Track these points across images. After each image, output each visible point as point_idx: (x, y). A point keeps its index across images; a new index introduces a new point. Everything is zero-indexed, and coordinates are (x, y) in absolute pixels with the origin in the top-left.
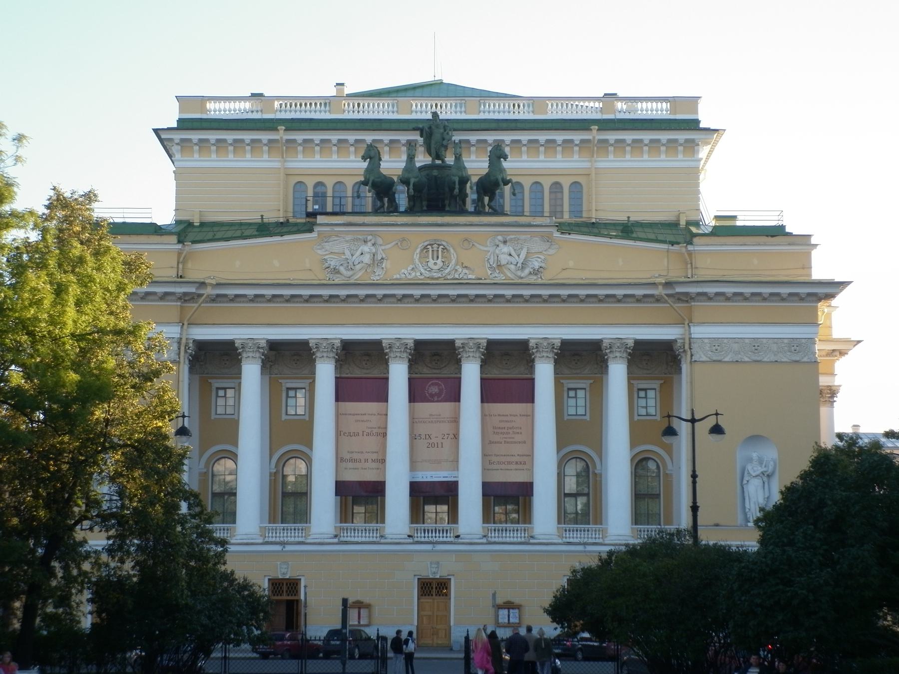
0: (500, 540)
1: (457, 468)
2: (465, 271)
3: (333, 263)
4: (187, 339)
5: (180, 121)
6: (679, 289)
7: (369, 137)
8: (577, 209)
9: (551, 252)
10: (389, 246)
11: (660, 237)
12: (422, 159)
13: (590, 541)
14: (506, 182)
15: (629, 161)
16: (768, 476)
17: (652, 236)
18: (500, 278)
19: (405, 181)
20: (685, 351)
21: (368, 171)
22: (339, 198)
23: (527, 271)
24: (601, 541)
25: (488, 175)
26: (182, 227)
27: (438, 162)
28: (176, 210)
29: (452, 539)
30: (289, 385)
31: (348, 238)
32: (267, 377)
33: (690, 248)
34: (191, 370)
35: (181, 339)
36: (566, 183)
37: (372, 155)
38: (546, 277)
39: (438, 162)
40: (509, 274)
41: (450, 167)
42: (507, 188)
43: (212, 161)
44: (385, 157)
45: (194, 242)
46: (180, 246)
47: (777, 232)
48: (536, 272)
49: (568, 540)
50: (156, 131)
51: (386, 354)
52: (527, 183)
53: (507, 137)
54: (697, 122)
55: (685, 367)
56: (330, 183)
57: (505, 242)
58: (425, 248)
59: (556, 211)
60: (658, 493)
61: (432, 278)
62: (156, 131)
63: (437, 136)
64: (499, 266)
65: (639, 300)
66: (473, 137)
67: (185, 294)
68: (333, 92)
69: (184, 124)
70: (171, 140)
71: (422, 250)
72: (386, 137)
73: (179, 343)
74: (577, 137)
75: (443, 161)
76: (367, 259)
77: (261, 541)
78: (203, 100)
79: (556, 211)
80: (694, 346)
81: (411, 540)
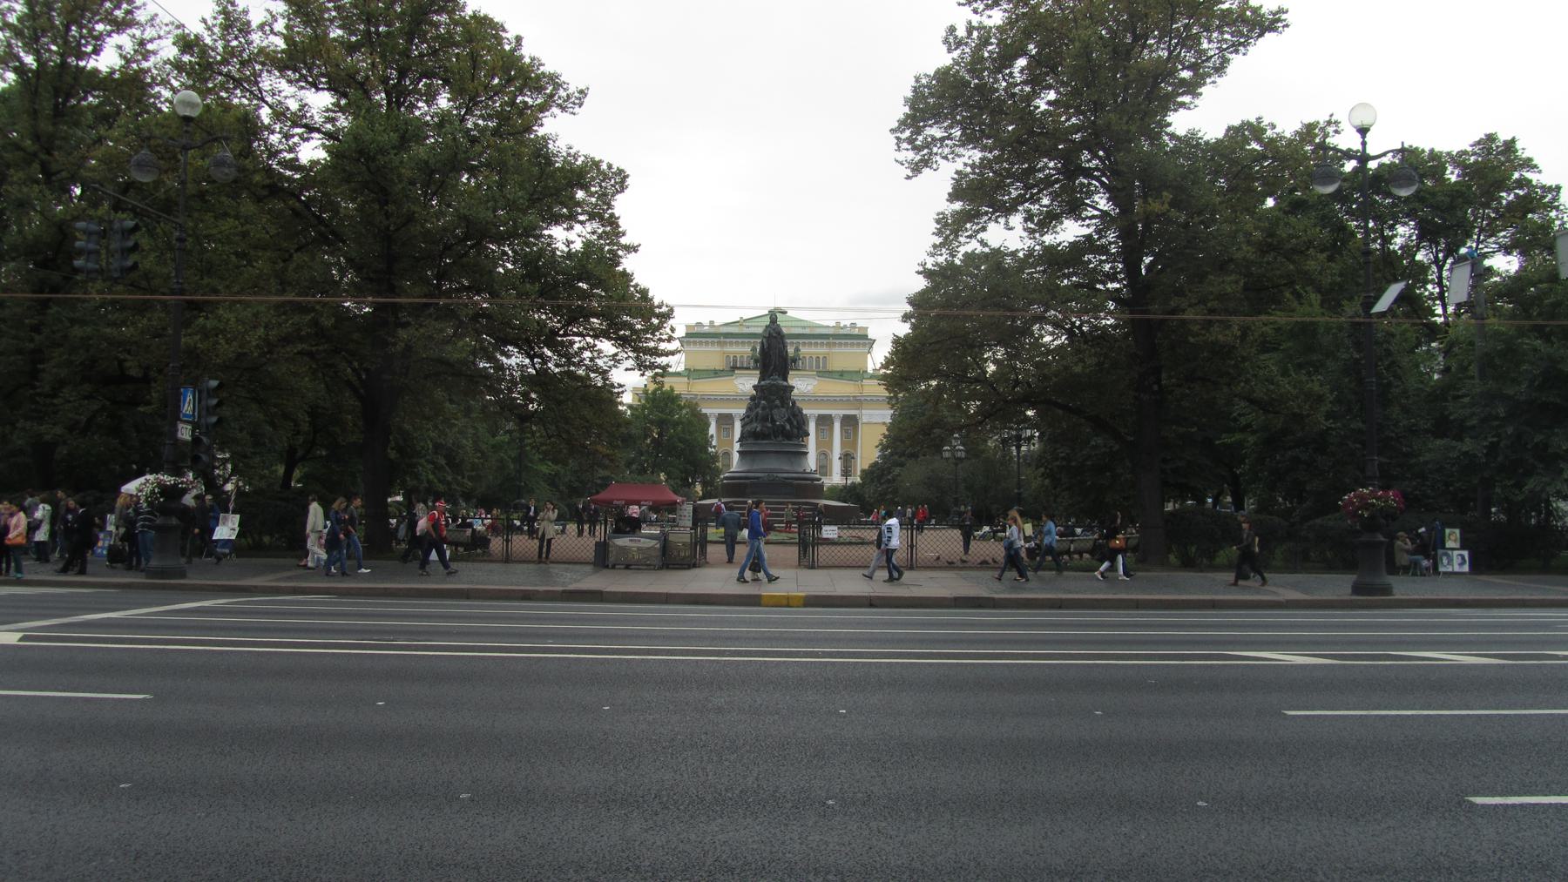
15: (844, 350)
22: (742, 362)
36: (821, 357)
43: (697, 348)
56: (738, 356)
59: (818, 366)
79: (818, 366)
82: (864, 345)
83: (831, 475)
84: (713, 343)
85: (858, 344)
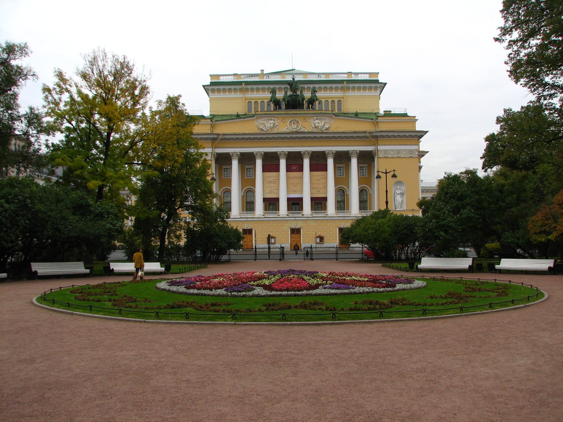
0: (317, 216)
1: (302, 193)
2: (304, 129)
3: (261, 127)
4: (214, 152)
5: (211, 83)
6: (374, 134)
7: (272, 87)
8: (340, 108)
9: (332, 122)
10: (279, 121)
11: (367, 117)
12: (289, 93)
13: (346, 216)
14: (317, 100)
15: (356, 93)
16: (403, 194)
17: (365, 117)
18: (315, 130)
19: (284, 100)
20: (376, 154)
21: (272, 98)
23: (324, 128)
24: (349, 216)
25: (311, 98)
26: (212, 116)
27: (295, 94)
28: (210, 111)
29: (301, 216)
30: (247, 167)
31: (266, 119)
32: (240, 165)
33: (377, 121)
34: (216, 163)
35: (212, 152)
36: (336, 100)
37: (273, 92)
38: (331, 130)
39: (295, 94)
40: (318, 130)
41: (298, 96)
42: (317, 102)
43: (221, 95)
44: (277, 93)
45: (216, 121)
46: (211, 123)
47: (405, 115)
48: (327, 129)
49: (338, 216)
50: (204, 86)
51: (279, 156)
52: (323, 100)
53: (317, 86)
54: (378, 80)
55: (376, 160)
56: (259, 101)
57: (317, 119)
58: (291, 121)
60: (366, 200)
61: (294, 131)
62: (204, 86)
63: (294, 85)
64: (315, 127)
65: (360, 137)
66: (306, 86)
67: (213, 138)
68: (260, 72)
69: (212, 84)
70: (208, 89)
71: (290, 122)
72: (277, 86)
73: (212, 154)
74: (339, 86)
75: (296, 93)
76: (272, 125)
77: (239, 217)
78: (219, 76)
80: (379, 152)
81: (288, 216)
82: (376, 89)
83: (348, 209)
84: (235, 90)
85: (370, 89)
